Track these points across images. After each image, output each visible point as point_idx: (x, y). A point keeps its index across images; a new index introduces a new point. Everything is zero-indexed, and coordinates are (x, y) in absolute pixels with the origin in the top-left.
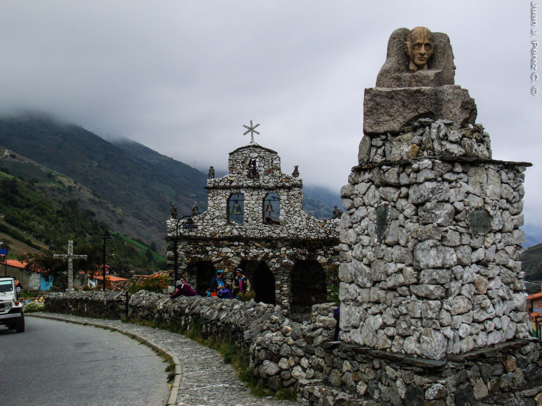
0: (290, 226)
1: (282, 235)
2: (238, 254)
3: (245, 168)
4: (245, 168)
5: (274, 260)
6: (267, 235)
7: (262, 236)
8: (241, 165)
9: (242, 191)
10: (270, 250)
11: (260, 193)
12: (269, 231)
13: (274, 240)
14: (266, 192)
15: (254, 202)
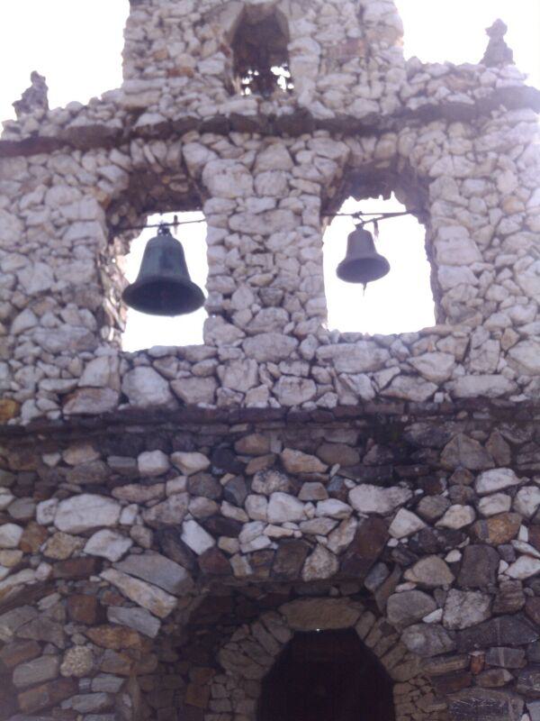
0: (516, 324)
1: (470, 386)
2: (165, 538)
3: (211, 47)
4: (211, 47)
5: (427, 569)
6: (367, 391)
7: (330, 401)
8: (189, 35)
9: (195, 153)
10: (400, 494)
11: (304, 157)
12: (383, 367)
13: (419, 415)
14: (341, 149)
15: (267, 203)
